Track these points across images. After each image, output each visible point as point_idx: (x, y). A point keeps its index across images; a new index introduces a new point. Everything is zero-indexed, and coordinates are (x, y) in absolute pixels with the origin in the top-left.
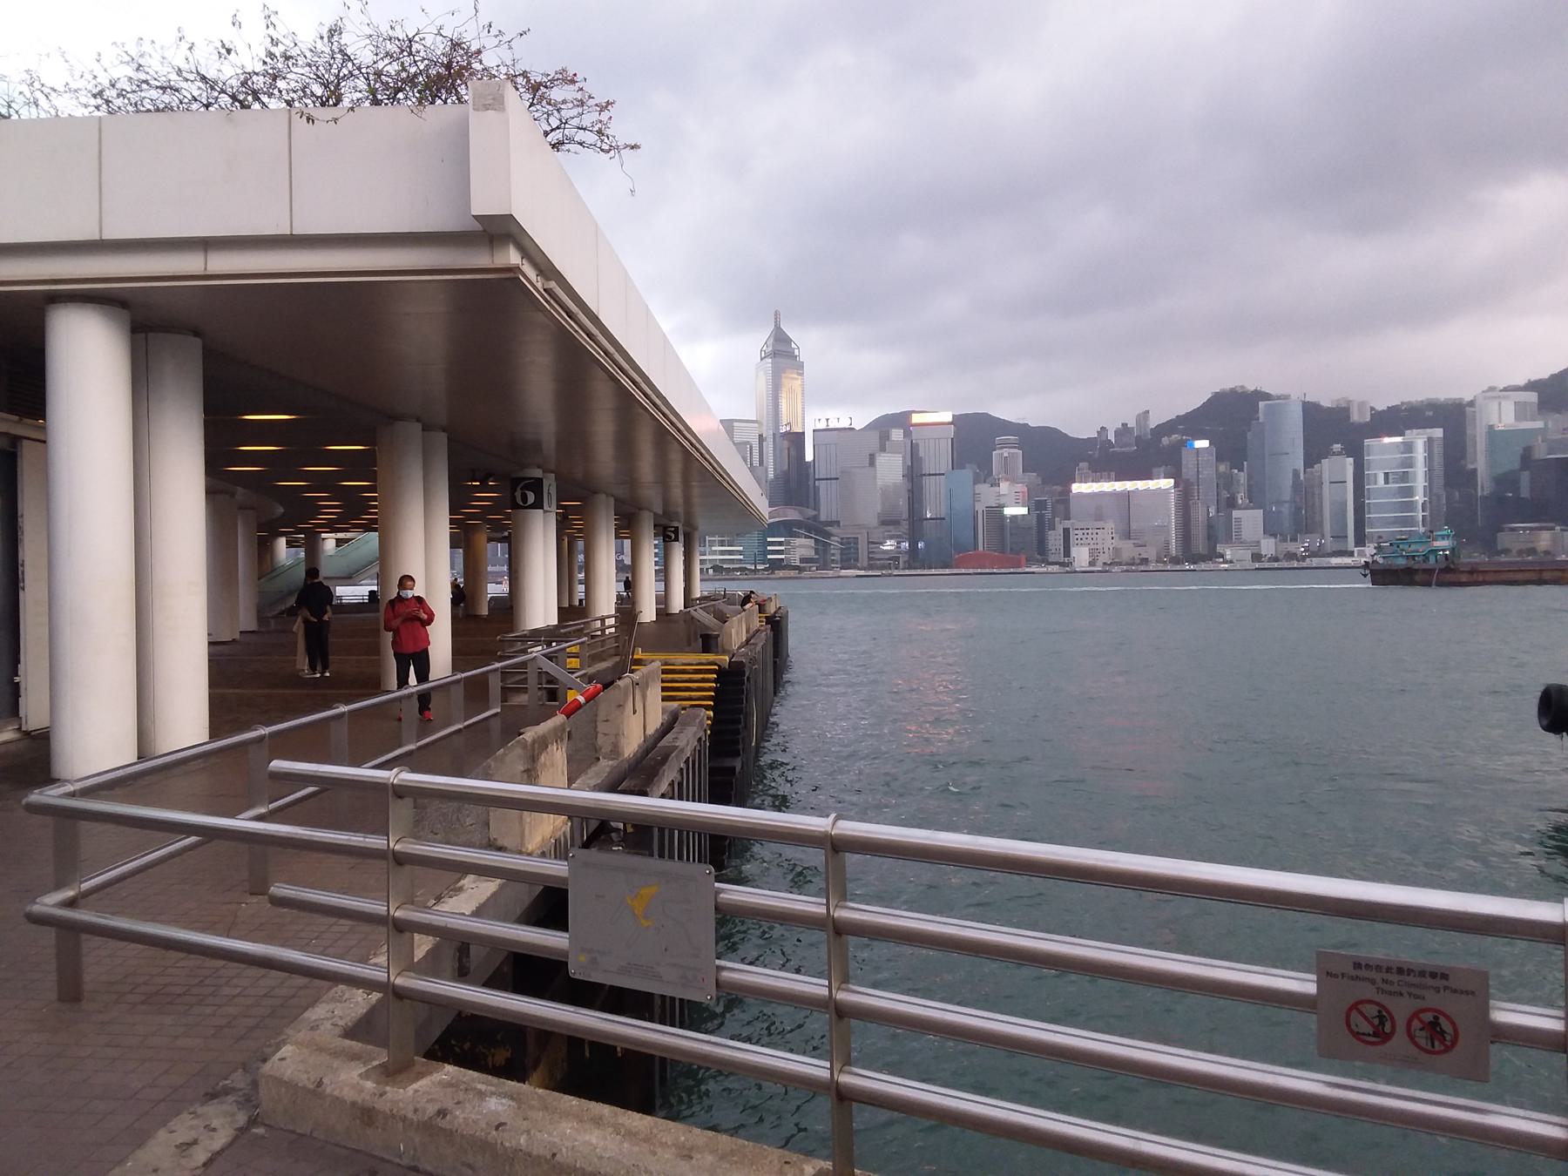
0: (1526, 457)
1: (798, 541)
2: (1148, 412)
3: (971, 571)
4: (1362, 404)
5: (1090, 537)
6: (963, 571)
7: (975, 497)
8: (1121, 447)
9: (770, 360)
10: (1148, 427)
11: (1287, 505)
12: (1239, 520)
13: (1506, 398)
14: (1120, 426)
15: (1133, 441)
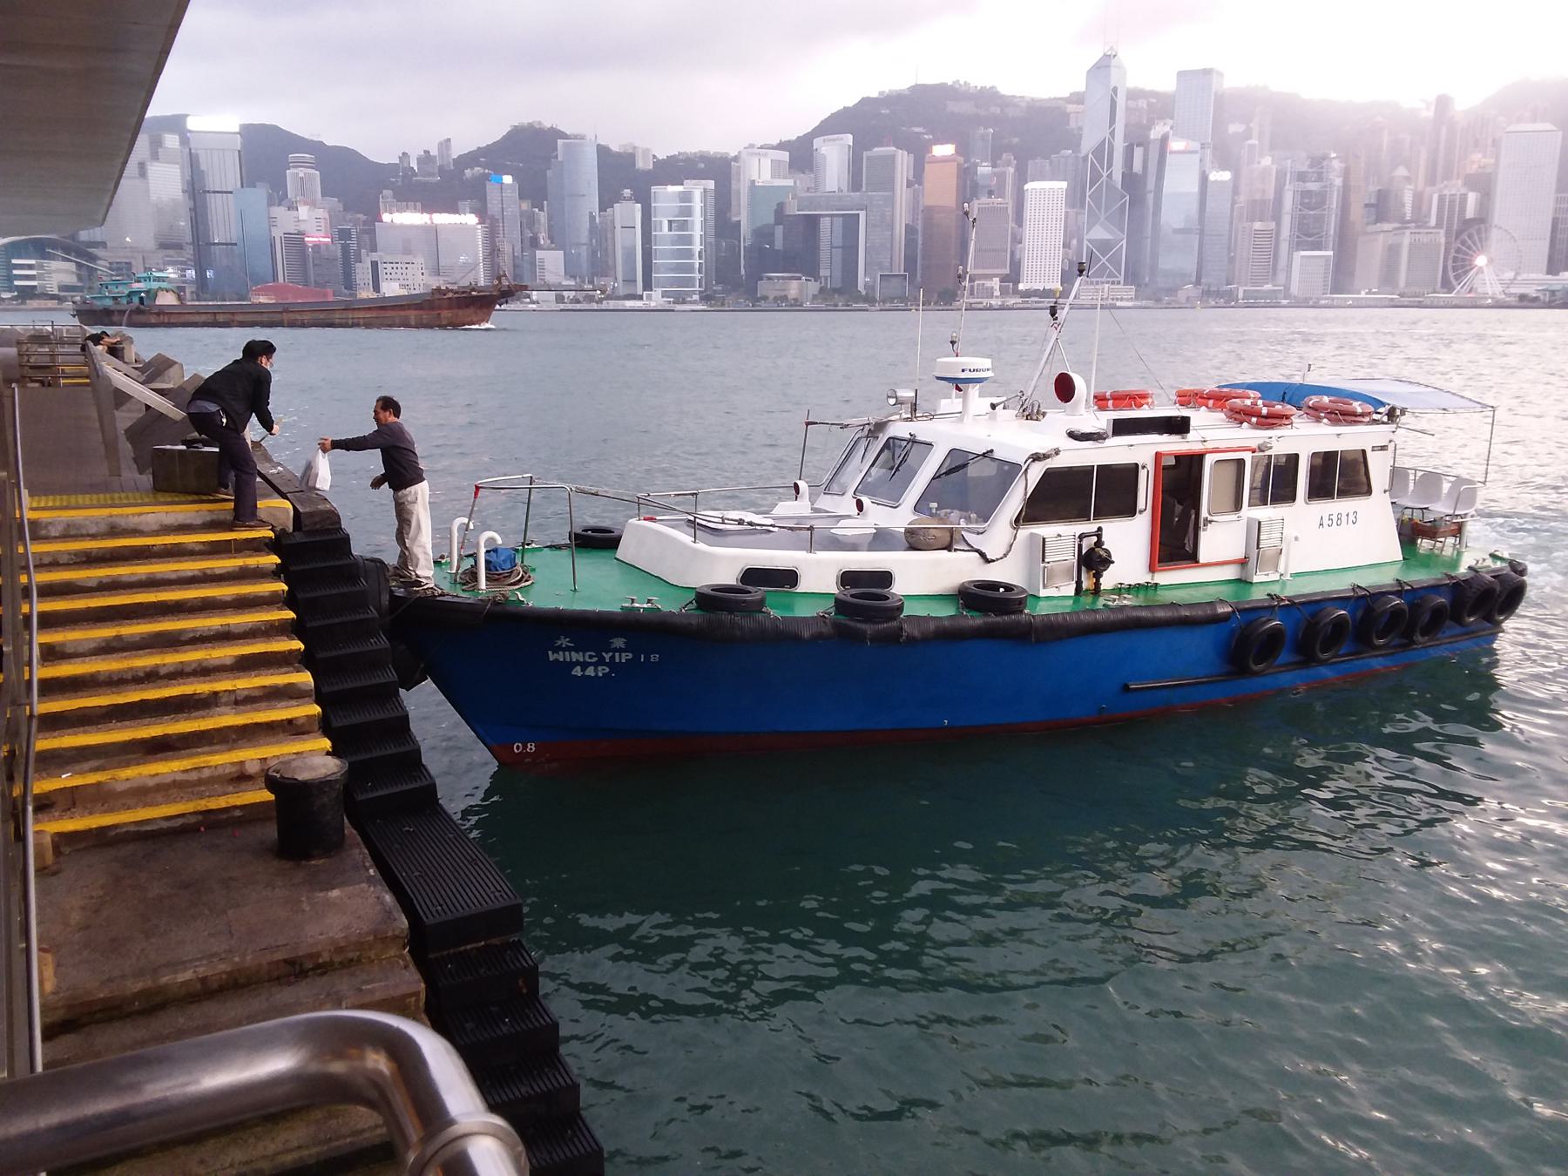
0: (780, 211)
1: (55, 265)
2: (449, 140)
4: (646, 151)
5: (399, 271)
7: (272, 221)
10: (449, 156)
11: (585, 247)
13: (766, 155)
15: (437, 171)
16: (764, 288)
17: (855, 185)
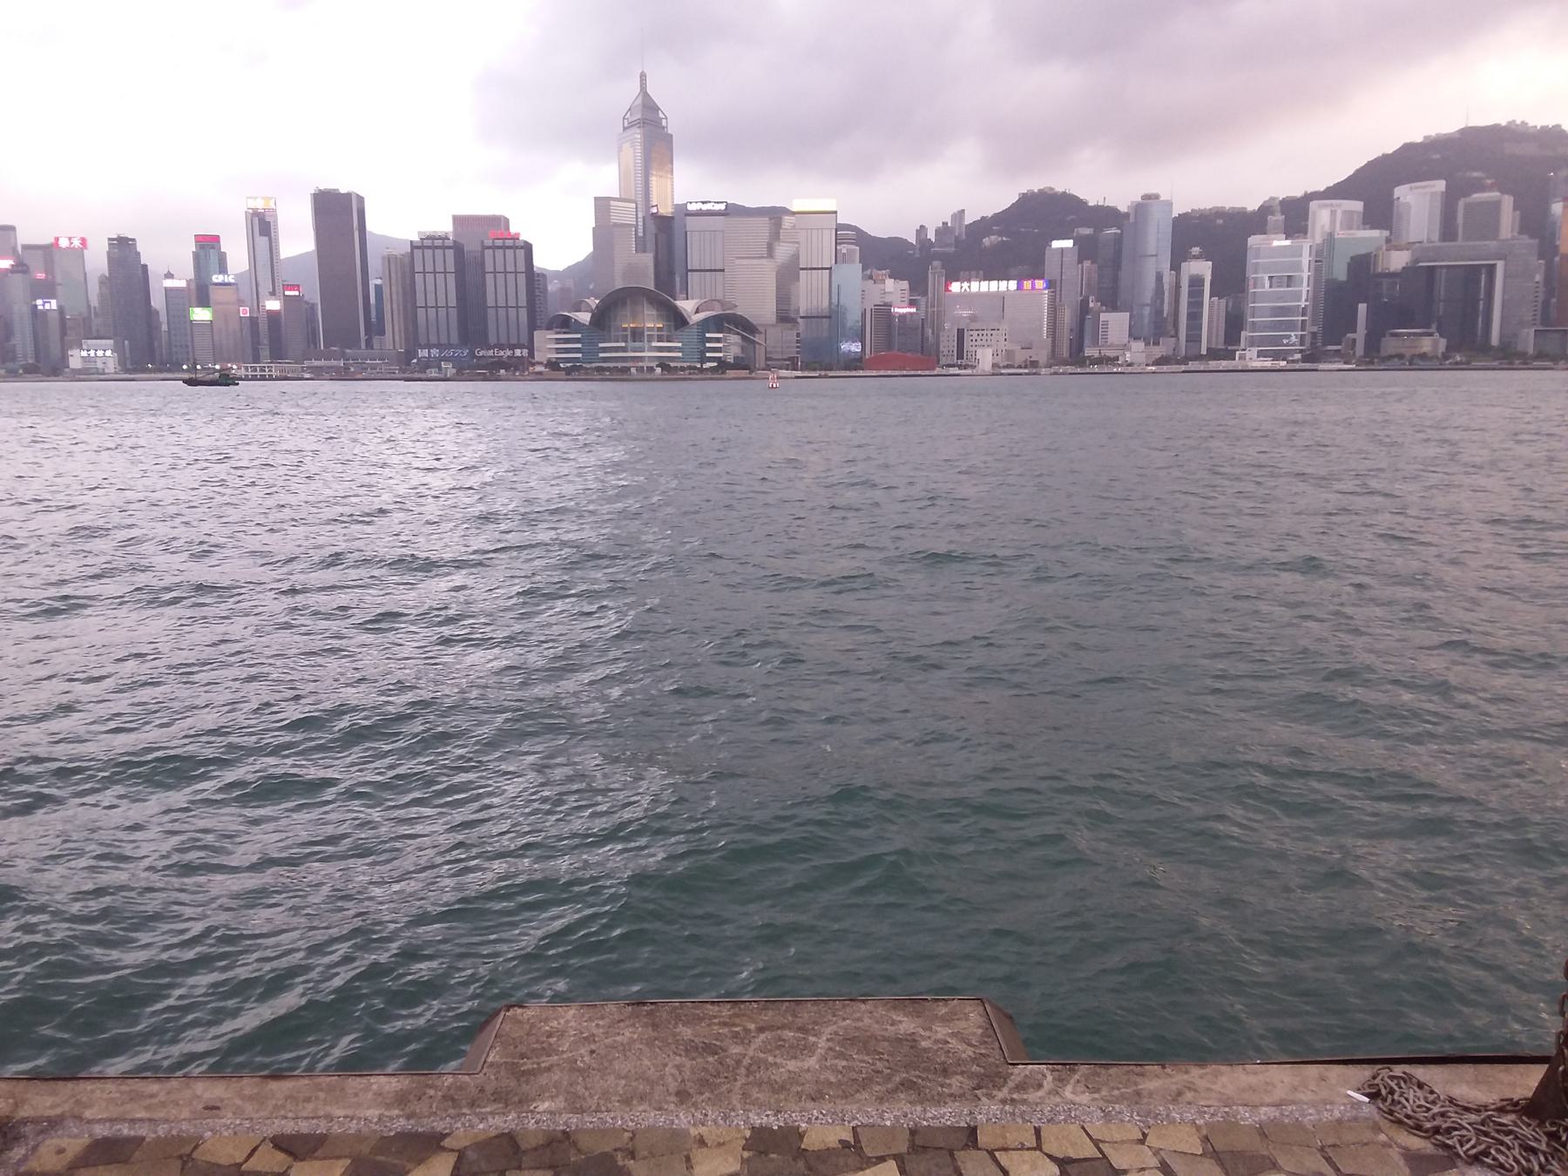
2: (963, 211)
3: (897, 373)
6: (889, 373)
8: (941, 247)
9: (638, 131)
12: (1106, 323)
13: (1339, 206)
14: (941, 225)
15: (953, 241)
16: (1390, 345)
17: (1448, 232)
